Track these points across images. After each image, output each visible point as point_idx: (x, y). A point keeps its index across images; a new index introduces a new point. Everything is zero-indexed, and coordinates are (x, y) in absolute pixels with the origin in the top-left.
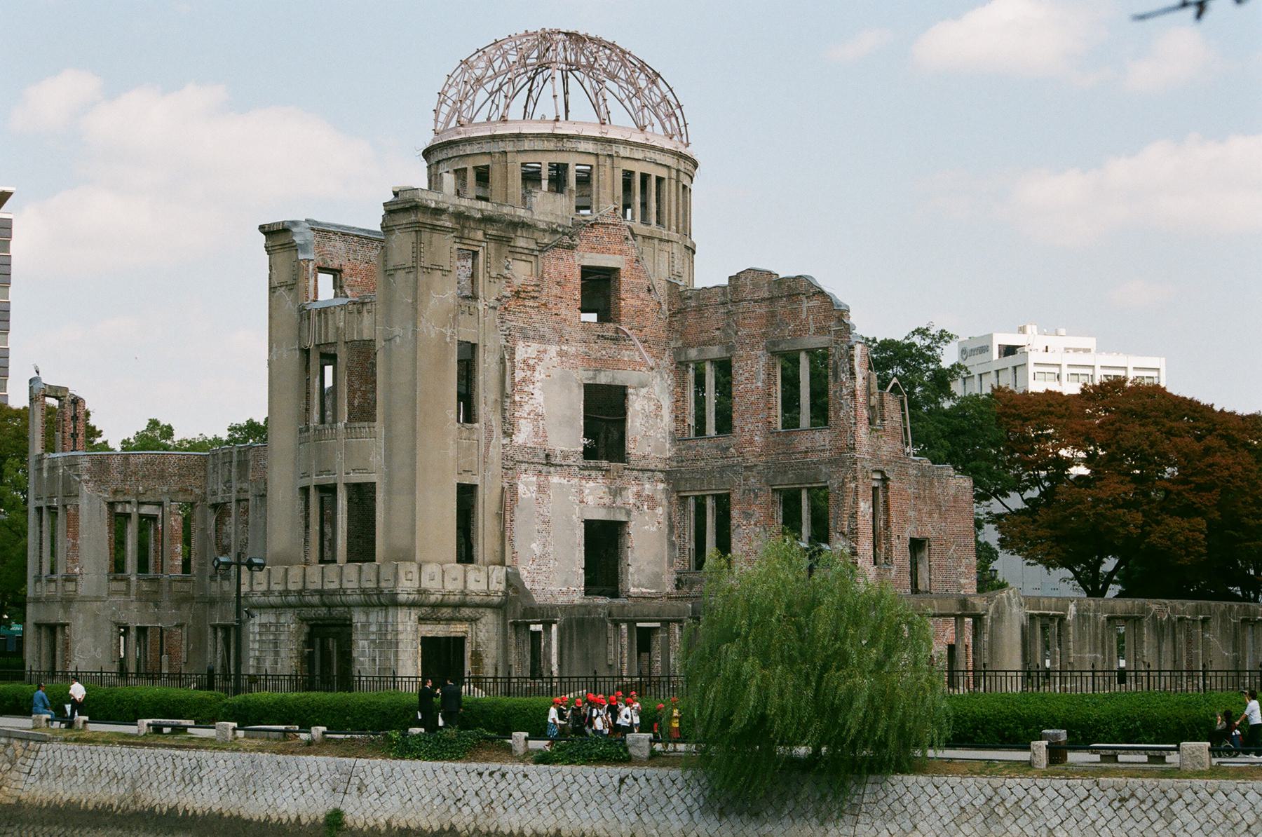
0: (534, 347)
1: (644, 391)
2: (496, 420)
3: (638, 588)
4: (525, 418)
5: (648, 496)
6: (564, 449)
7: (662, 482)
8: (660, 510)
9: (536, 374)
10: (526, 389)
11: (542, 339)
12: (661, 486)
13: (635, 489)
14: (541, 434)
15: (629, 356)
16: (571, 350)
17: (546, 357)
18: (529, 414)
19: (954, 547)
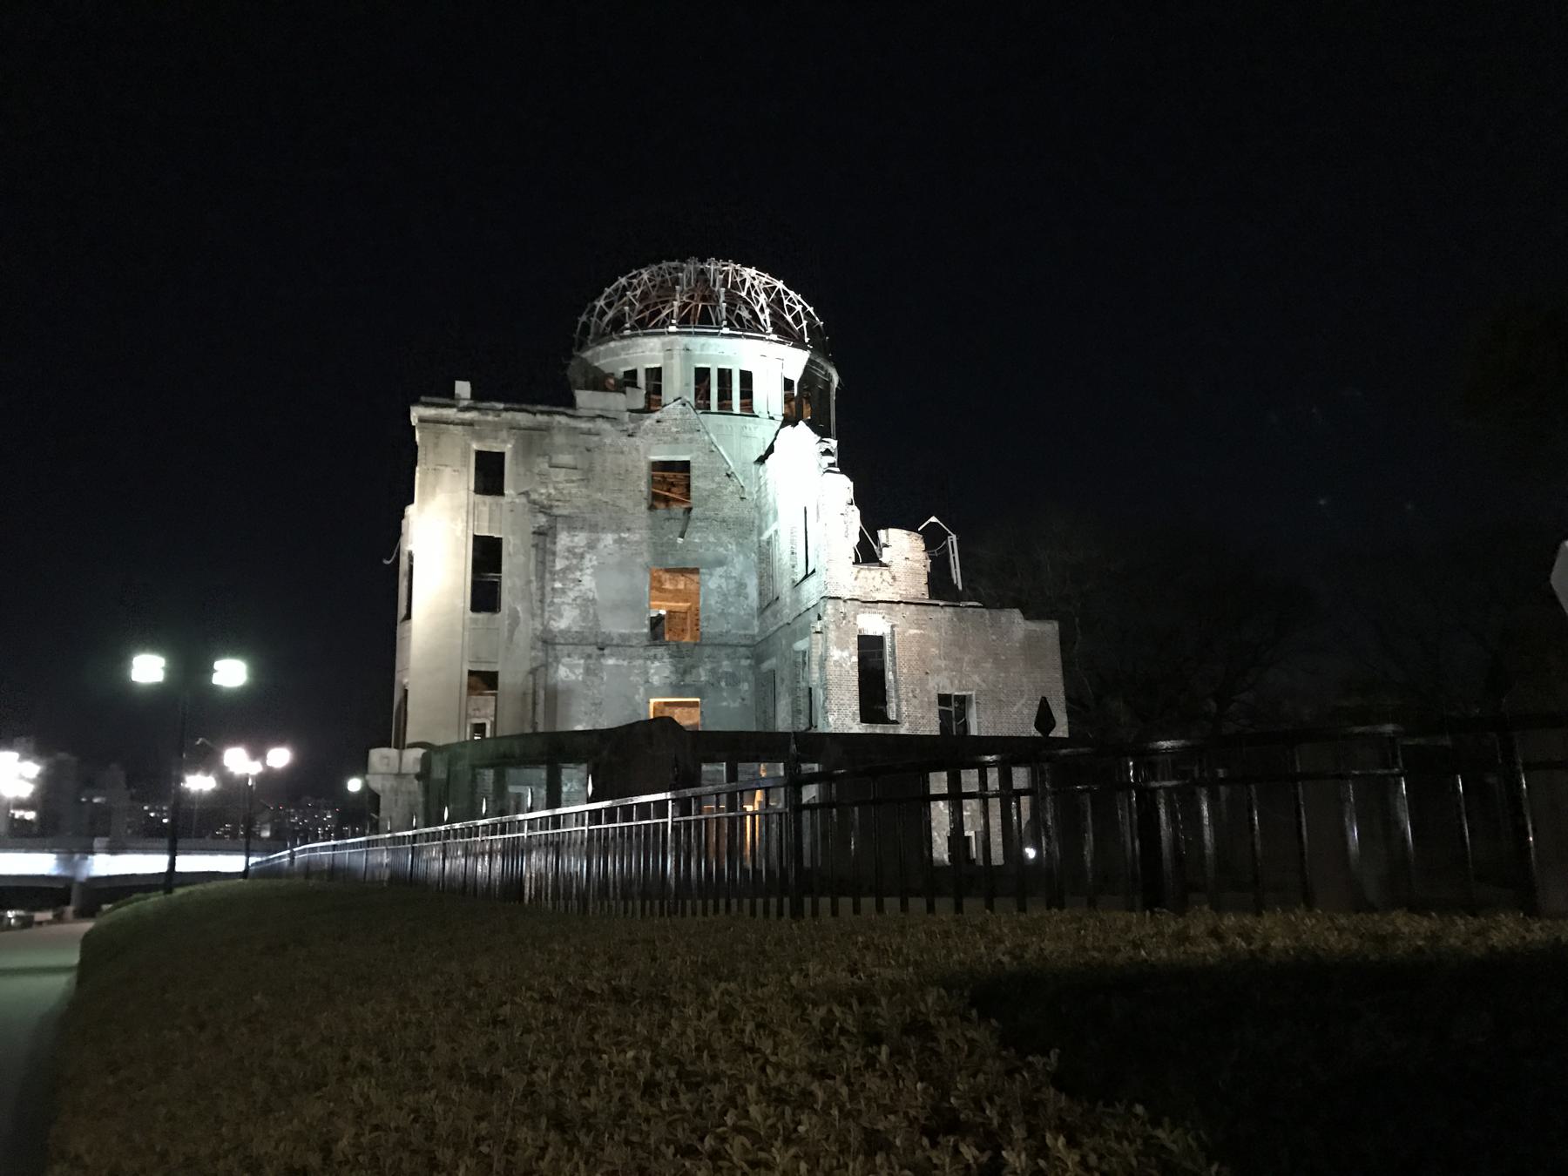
0: (581, 539)
1: (720, 571)
4: (569, 604)
5: (727, 673)
6: (623, 631)
7: (748, 658)
8: (745, 686)
9: (586, 562)
10: (571, 576)
11: (594, 528)
12: (745, 663)
13: (708, 667)
14: (591, 617)
15: (700, 538)
16: (636, 537)
17: (601, 546)
18: (574, 600)
19: (1023, 701)
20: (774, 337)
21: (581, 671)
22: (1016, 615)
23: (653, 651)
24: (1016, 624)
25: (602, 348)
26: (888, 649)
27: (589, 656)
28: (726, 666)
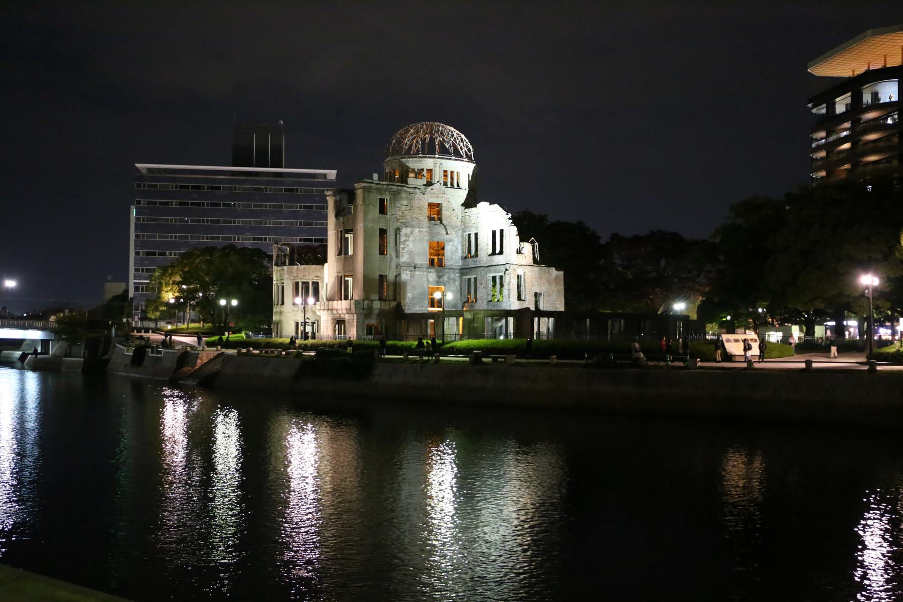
0: (409, 230)
1: (451, 243)
2: (393, 254)
3: (448, 308)
9: (410, 239)
11: (412, 227)
13: (447, 276)
14: (412, 258)
17: (414, 233)
20: (466, 160)
21: (409, 276)
22: (554, 269)
23: (429, 270)
24: (554, 272)
25: (411, 159)
26: (523, 279)
27: (412, 271)
28: (452, 276)
